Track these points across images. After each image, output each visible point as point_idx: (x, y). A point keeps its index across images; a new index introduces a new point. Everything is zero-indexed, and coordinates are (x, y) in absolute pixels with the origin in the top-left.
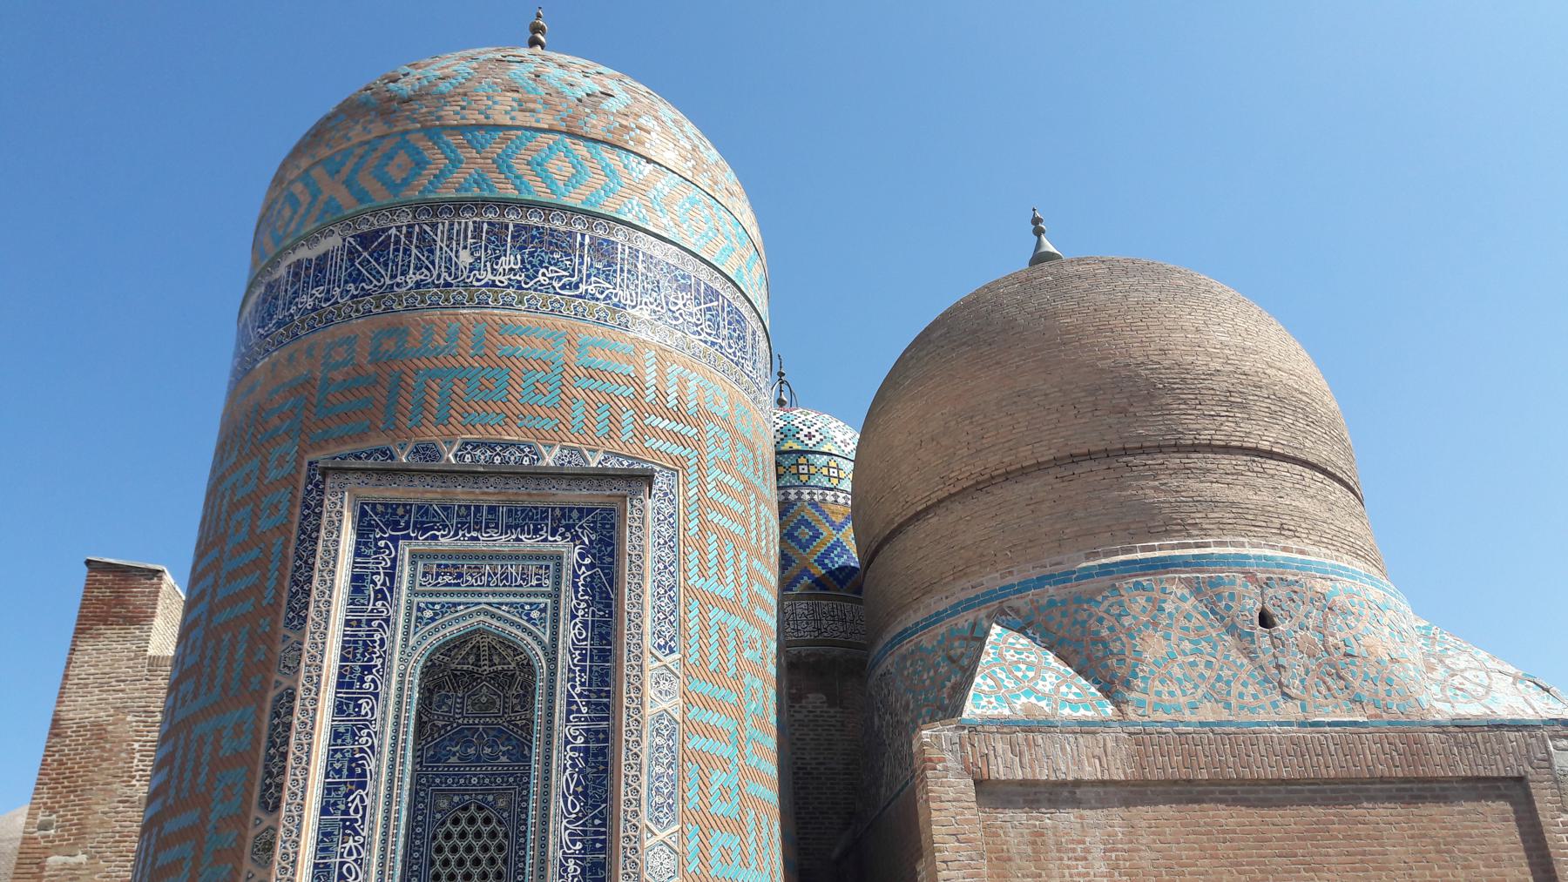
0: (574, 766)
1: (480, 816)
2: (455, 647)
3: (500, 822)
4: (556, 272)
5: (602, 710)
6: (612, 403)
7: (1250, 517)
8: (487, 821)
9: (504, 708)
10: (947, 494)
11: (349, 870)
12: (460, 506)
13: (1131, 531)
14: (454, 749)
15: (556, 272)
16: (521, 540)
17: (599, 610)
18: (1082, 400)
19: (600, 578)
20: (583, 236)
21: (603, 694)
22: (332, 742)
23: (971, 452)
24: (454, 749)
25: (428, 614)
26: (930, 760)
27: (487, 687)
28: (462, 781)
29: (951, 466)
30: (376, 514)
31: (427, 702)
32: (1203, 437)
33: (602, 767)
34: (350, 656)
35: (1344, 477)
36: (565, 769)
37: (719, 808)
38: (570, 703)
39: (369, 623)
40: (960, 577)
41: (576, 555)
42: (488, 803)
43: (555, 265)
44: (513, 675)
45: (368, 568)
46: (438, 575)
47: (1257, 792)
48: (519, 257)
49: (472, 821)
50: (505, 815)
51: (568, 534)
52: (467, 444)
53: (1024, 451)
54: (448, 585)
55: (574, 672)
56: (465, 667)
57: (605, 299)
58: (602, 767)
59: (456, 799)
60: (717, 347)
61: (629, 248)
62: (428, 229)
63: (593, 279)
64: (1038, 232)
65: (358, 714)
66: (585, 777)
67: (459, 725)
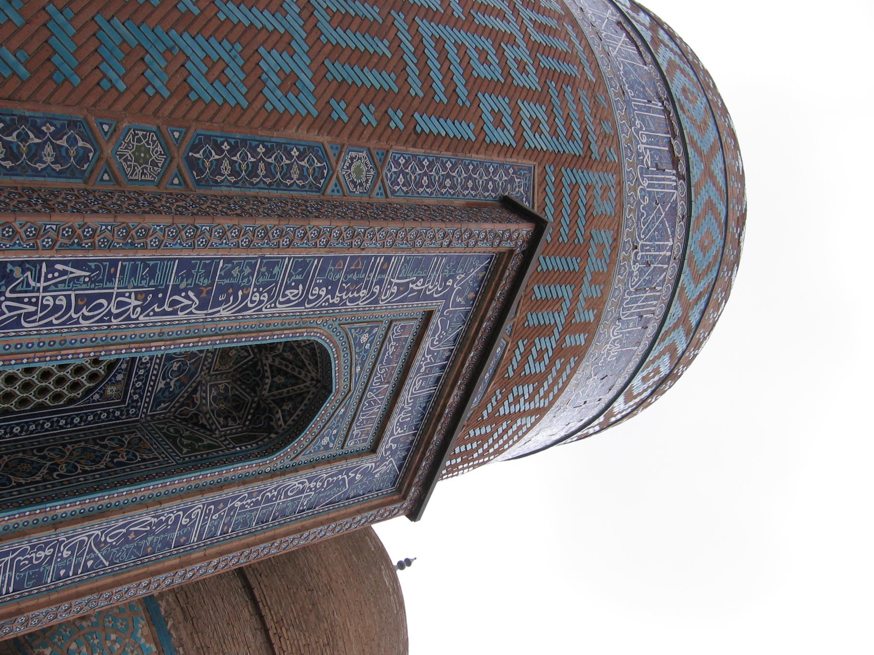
0: (160, 523)
10: (268, 626)
11: (101, 306)
22: (265, 261)
23: (302, 648)
27: (246, 357)
29: (292, 627)
36: (158, 517)
39: (380, 282)
42: (115, 376)
45: (433, 272)
50: (96, 397)
54: (386, 350)
65: (288, 287)
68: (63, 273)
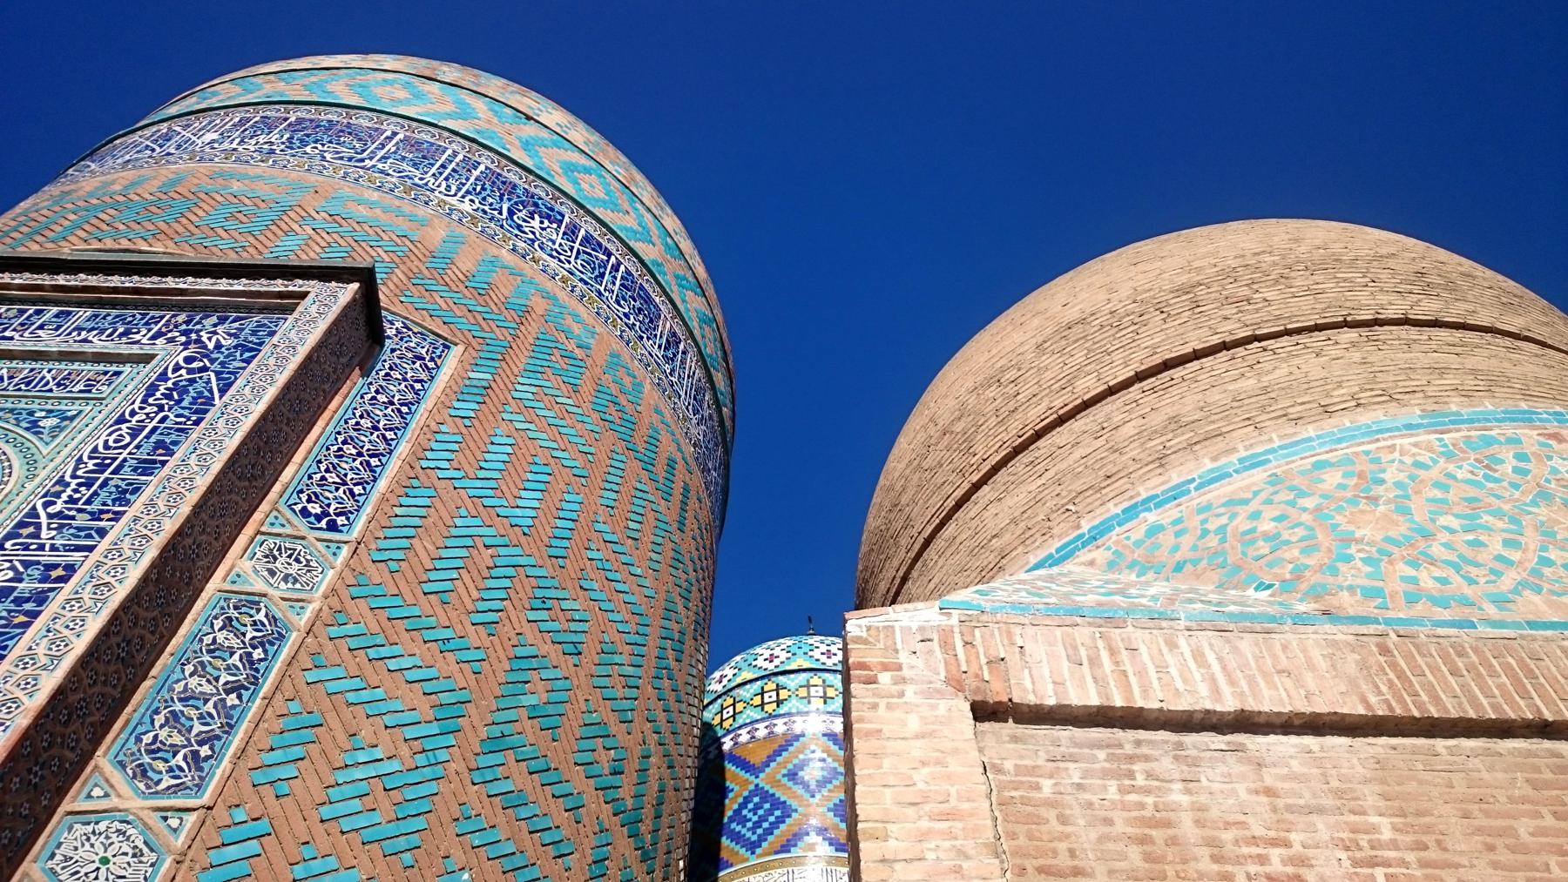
13: (1291, 417)
16: (91, 342)
18: (1172, 302)
20: (394, 134)
26: (863, 666)
29: (971, 451)
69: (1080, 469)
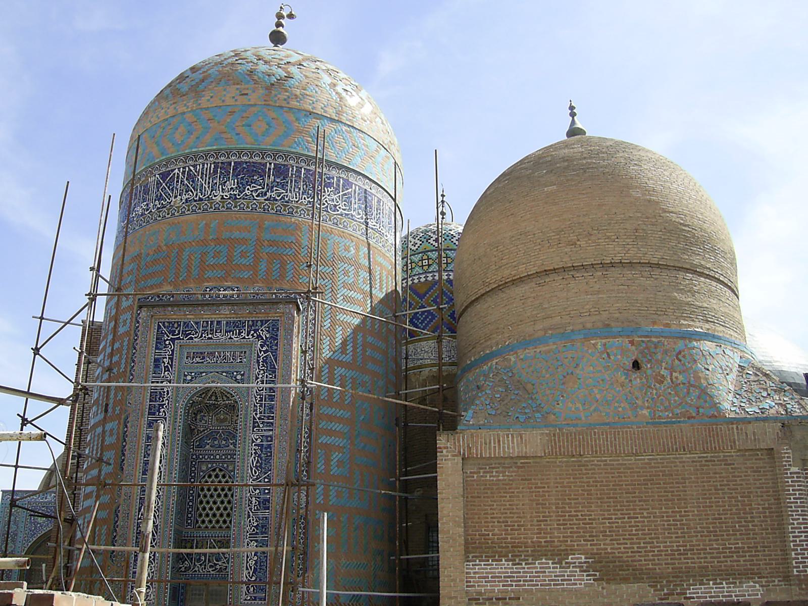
1: (221, 474)
2: (203, 393)
3: (230, 477)
4: (255, 187)
5: (270, 426)
6: (282, 259)
7: (638, 305)
8: (224, 476)
9: (232, 421)
10: (485, 292)
12: (203, 322)
13: (571, 316)
14: (208, 442)
15: (255, 187)
16: (232, 339)
17: (270, 374)
19: (271, 357)
20: (270, 164)
21: (270, 418)
23: (497, 267)
24: (208, 442)
25: (189, 378)
26: (440, 448)
28: (212, 457)
30: (165, 328)
31: (194, 419)
32: (616, 258)
33: (269, 454)
34: (154, 399)
35: (712, 274)
36: (252, 454)
37: (334, 470)
38: (254, 423)
40: (488, 340)
41: (259, 345)
43: (254, 183)
44: (234, 406)
46: (193, 358)
47: (618, 460)
48: (236, 181)
49: (217, 476)
50: (232, 473)
51: (255, 335)
52: (207, 288)
53: (522, 268)
54: (198, 363)
55: (257, 406)
56: (211, 402)
57: (281, 199)
58: (269, 454)
59: (210, 466)
60: (350, 216)
61: (296, 167)
62: (192, 168)
63: (275, 188)
64: (573, 115)
66: (261, 459)
67: (210, 430)
68: (142, 515)
69: (514, 312)
